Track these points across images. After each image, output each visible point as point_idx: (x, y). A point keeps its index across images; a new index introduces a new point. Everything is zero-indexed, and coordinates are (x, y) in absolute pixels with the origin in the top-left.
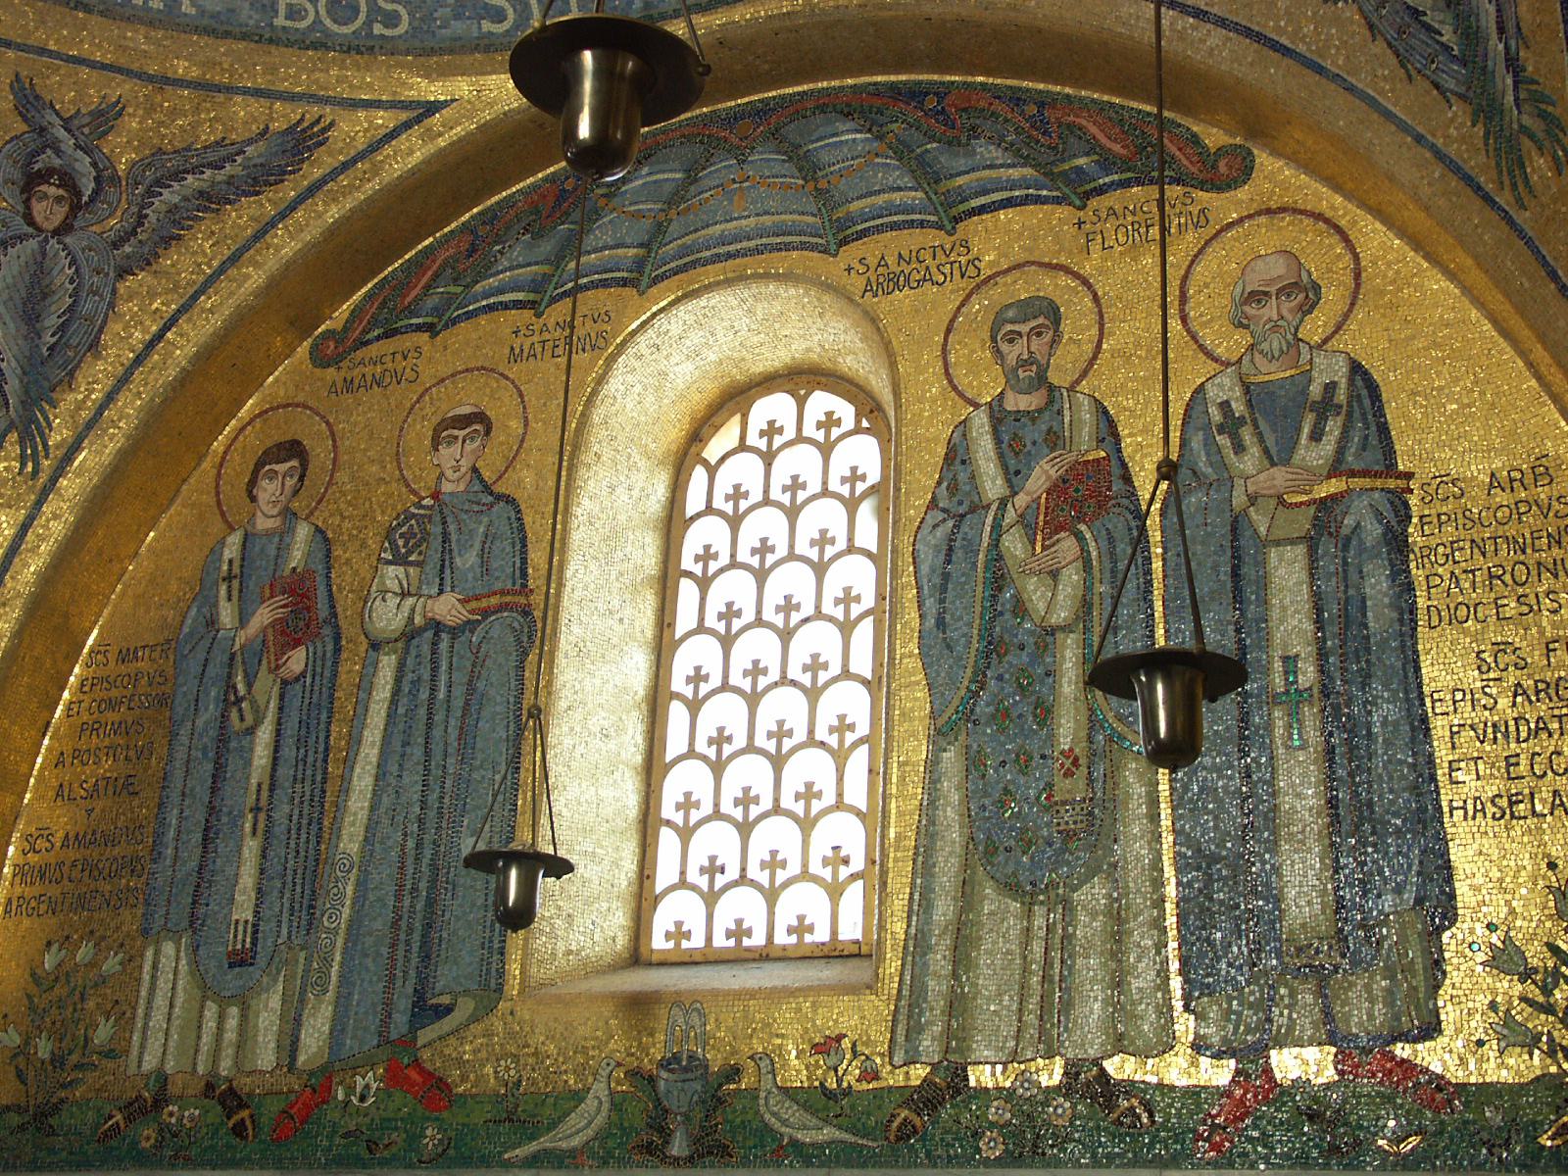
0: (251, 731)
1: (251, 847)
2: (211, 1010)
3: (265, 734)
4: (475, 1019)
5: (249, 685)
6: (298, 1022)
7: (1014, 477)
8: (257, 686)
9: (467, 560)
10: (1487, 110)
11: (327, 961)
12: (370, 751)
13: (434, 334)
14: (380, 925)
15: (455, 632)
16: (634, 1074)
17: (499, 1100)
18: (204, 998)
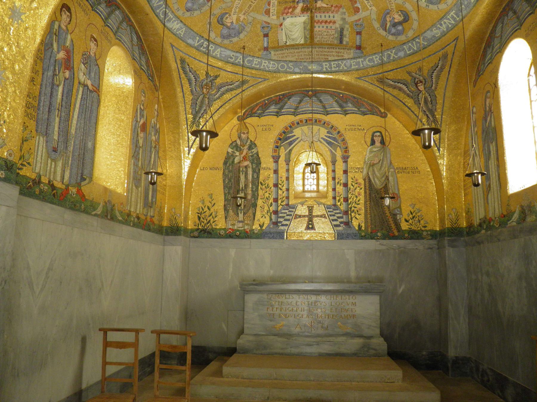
0: (58, 86)
1: (57, 120)
2: (49, 161)
3: (60, 89)
4: (88, 183)
5: (59, 73)
6: (64, 171)
7: (140, 119)
8: (60, 74)
9: (93, 75)
10: (194, 118)
11: (69, 159)
12: (77, 110)
13: (92, 10)
14: (77, 154)
15: (91, 91)
16: (105, 202)
17: (91, 201)
18: (48, 157)
